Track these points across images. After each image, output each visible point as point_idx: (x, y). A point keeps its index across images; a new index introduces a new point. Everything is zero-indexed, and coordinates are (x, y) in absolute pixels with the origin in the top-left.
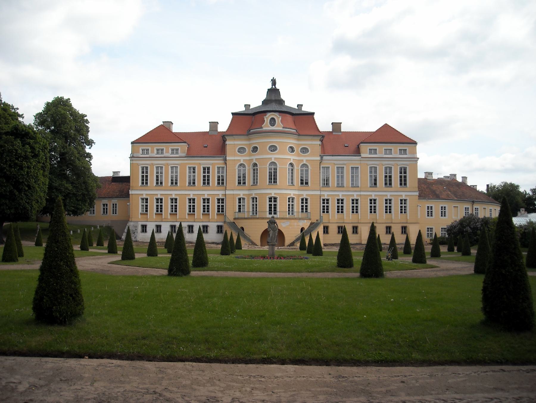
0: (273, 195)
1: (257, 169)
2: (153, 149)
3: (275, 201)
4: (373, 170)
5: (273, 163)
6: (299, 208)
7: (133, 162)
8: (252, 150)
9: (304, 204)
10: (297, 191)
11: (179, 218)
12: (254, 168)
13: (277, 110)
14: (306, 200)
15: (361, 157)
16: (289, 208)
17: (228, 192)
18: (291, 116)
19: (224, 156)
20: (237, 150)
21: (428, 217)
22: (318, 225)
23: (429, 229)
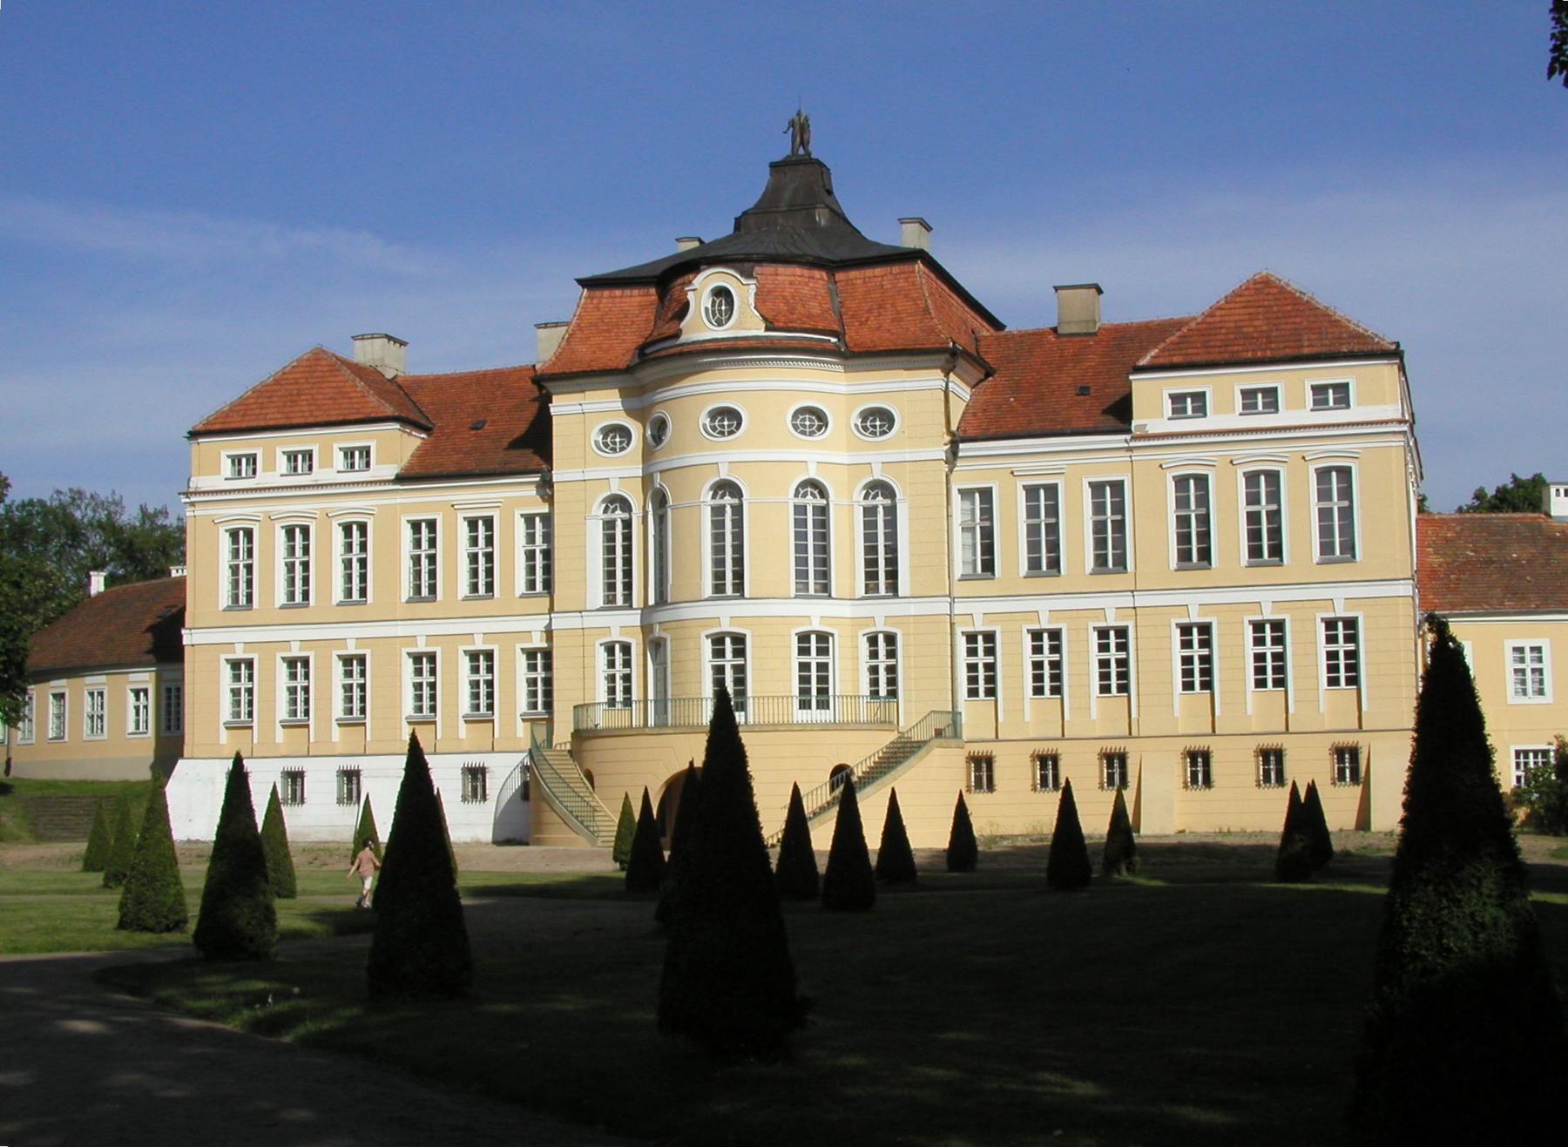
0: (726, 627)
2: (272, 449)
3: (740, 652)
4: (1193, 488)
5: (727, 487)
6: (856, 681)
7: (196, 513)
9: (882, 662)
11: (372, 741)
14: (891, 639)
15: (1128, 437)
17: (558, 622)
21: (1522, 700)
23: (1531, 755)
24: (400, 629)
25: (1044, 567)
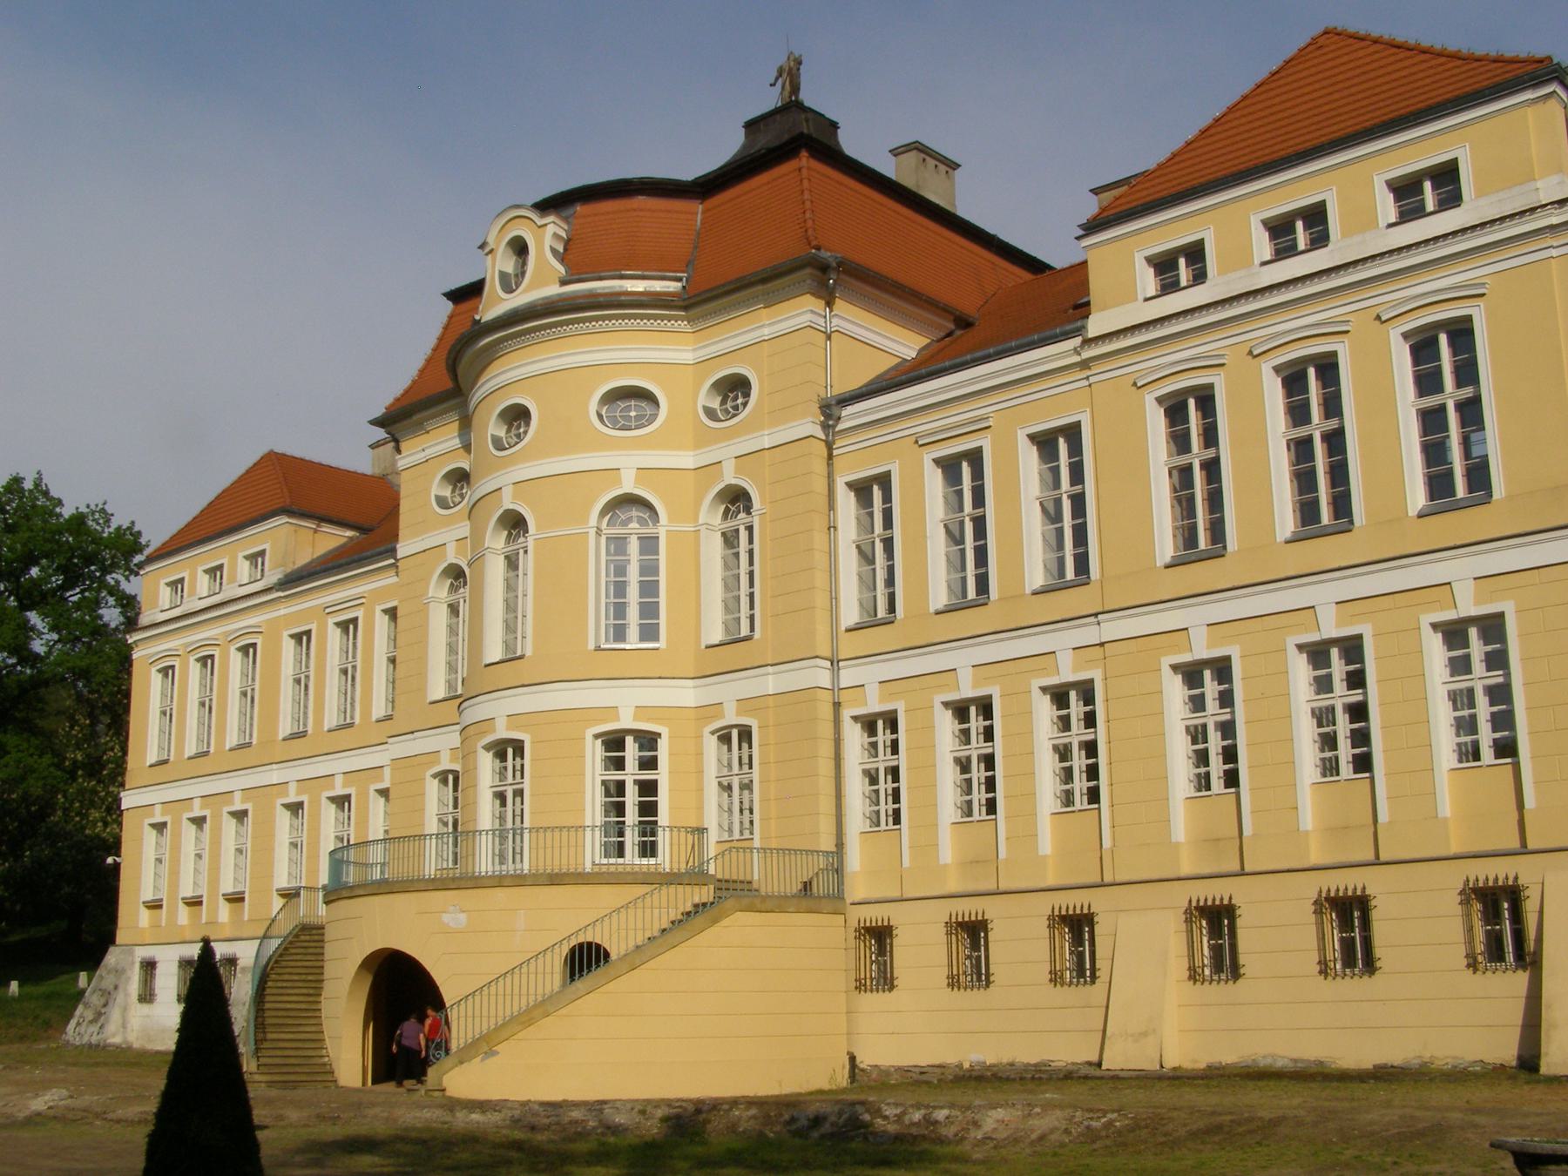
10: (690, 683)
24: (274, 775)
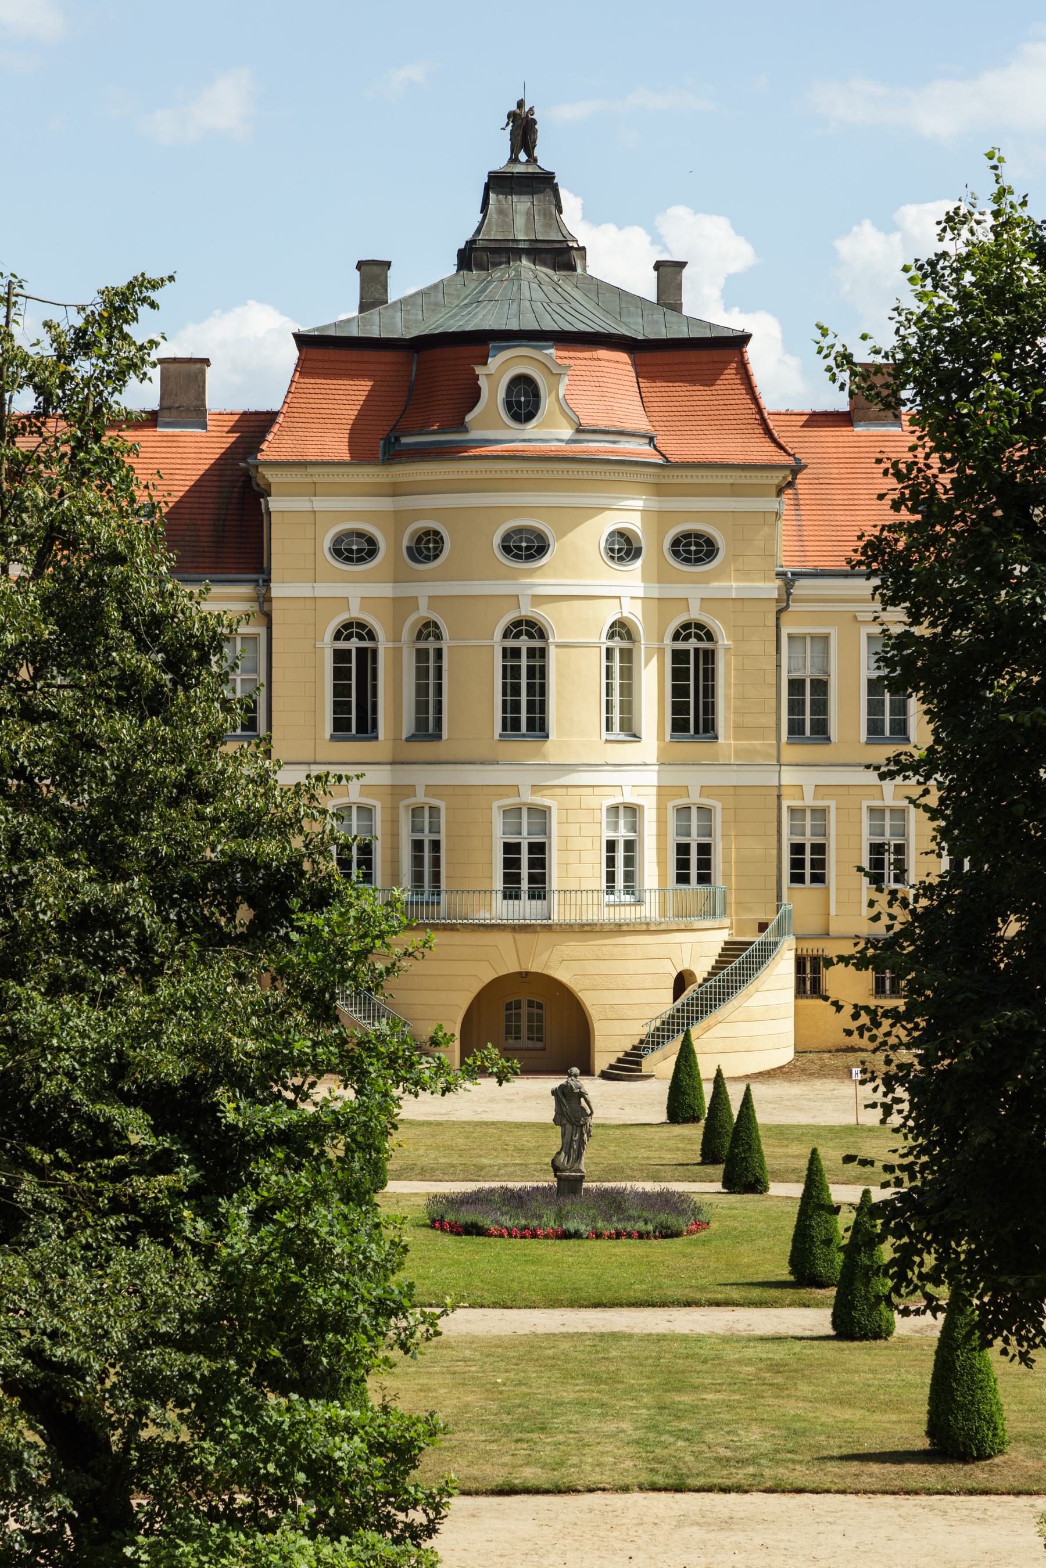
1: (439, 653)
8: (409, 549)
12: (422, 645)
13: (548, 325)
16: (611, 862)
18: (623, 357)
19: (254, 576)
20: (327, 543)
22: (767, 957)
25: (887, 733)
